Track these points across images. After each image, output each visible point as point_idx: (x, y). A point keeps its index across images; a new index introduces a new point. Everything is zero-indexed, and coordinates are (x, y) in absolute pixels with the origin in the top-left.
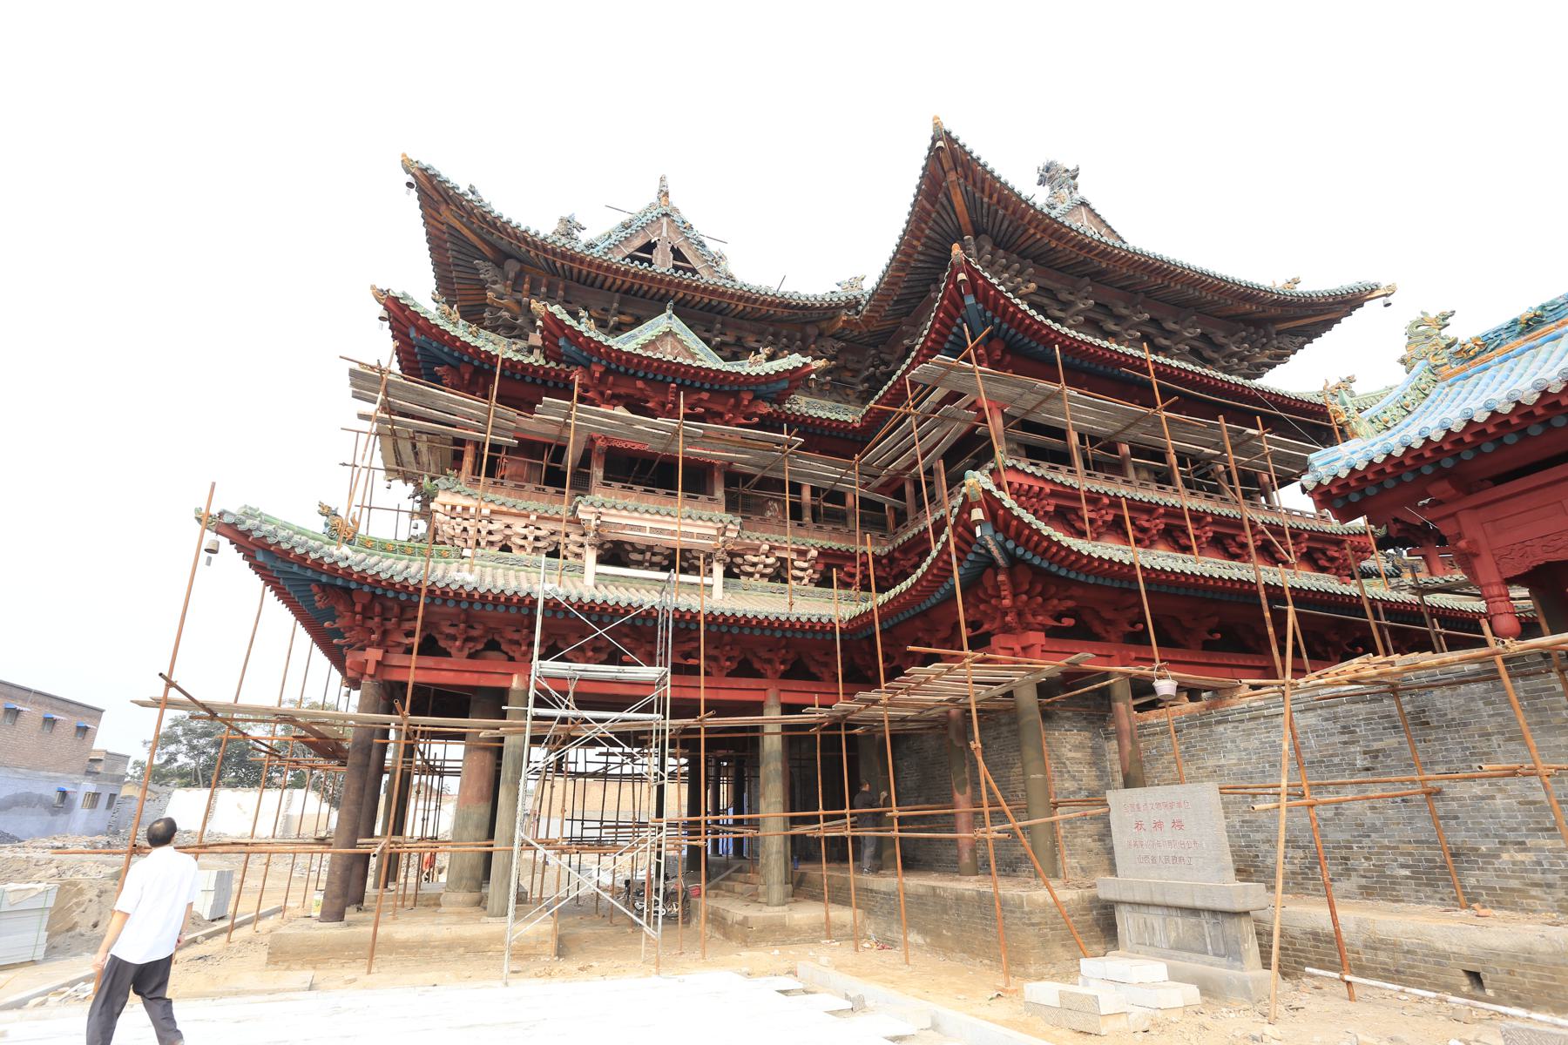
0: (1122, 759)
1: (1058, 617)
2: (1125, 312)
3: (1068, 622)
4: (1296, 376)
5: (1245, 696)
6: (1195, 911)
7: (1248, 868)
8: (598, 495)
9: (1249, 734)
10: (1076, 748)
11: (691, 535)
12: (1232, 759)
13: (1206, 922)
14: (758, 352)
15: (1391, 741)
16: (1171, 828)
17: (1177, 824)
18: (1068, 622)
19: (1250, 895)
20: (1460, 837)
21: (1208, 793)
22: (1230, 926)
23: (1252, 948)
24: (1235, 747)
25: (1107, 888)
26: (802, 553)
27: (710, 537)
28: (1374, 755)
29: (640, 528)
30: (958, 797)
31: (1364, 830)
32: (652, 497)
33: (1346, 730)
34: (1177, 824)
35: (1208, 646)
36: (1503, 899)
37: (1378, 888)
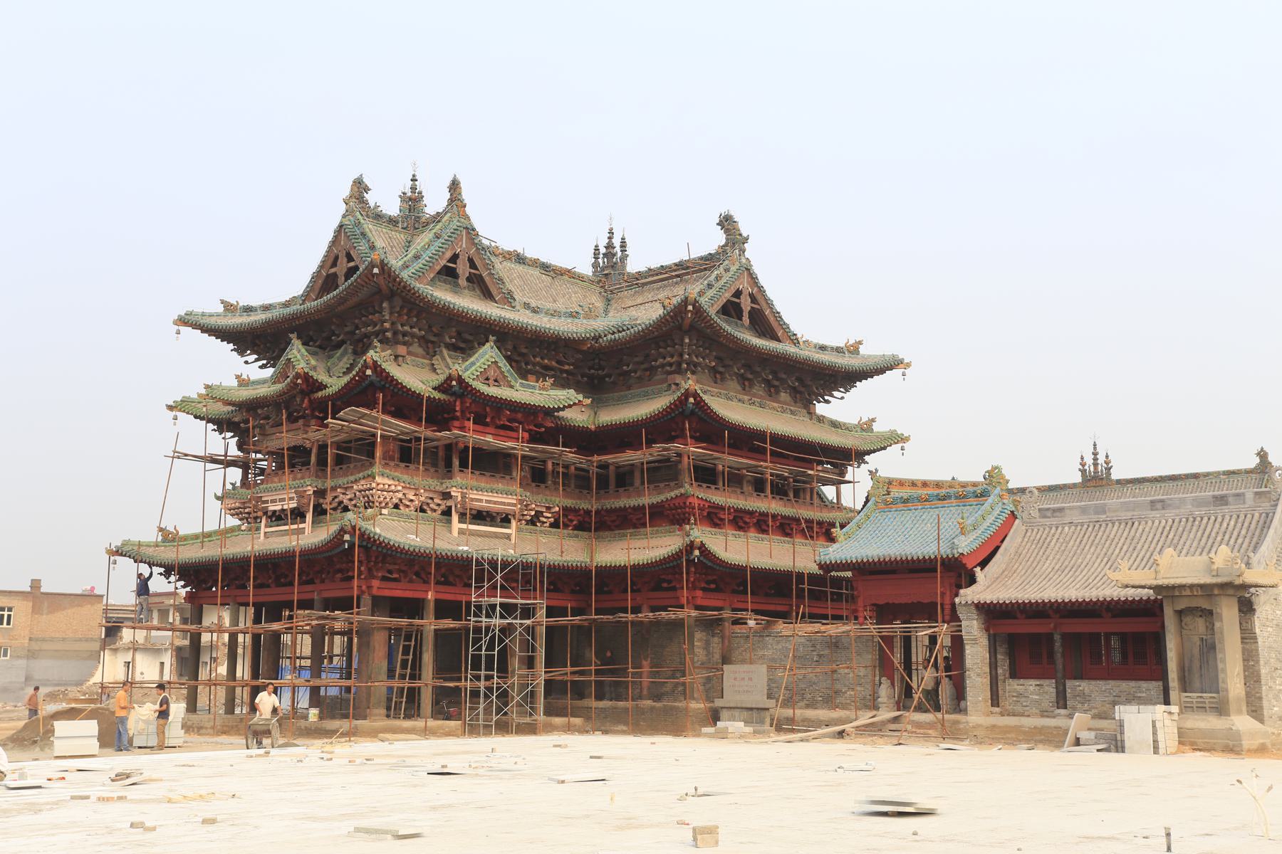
0: (722, 649)
1: (708, 582)
2: (758, 369)
3: (713, 586)
4: (843, 408)
5: (781, 627)
6: (751, 709)
7: (770, 697)
8: (459, 479)
9: (778, 642)
10: (699, 640)
11: (504, 504)
12: (768, 653)
13: (755, 714)
15: (826, 652)
16: (746, 681)
17: (750, 679)
18: (713, 586)
19: (771, 703)
20: (838, 686)
21: (762, 669)
22: (763, 713)
23: (768, 721)
24: (772, 648)
25: (718, 703)
26: (548, 508)
27: (509, 504)
28: (820, 656)
29: (481, 501)
30: (644, 663)
31: (812, 684)
32: (484, 478)
33: (813, 646)
34: (750, 679)
35: (767, 595)
36: (844, 707)
37: (812, 705)
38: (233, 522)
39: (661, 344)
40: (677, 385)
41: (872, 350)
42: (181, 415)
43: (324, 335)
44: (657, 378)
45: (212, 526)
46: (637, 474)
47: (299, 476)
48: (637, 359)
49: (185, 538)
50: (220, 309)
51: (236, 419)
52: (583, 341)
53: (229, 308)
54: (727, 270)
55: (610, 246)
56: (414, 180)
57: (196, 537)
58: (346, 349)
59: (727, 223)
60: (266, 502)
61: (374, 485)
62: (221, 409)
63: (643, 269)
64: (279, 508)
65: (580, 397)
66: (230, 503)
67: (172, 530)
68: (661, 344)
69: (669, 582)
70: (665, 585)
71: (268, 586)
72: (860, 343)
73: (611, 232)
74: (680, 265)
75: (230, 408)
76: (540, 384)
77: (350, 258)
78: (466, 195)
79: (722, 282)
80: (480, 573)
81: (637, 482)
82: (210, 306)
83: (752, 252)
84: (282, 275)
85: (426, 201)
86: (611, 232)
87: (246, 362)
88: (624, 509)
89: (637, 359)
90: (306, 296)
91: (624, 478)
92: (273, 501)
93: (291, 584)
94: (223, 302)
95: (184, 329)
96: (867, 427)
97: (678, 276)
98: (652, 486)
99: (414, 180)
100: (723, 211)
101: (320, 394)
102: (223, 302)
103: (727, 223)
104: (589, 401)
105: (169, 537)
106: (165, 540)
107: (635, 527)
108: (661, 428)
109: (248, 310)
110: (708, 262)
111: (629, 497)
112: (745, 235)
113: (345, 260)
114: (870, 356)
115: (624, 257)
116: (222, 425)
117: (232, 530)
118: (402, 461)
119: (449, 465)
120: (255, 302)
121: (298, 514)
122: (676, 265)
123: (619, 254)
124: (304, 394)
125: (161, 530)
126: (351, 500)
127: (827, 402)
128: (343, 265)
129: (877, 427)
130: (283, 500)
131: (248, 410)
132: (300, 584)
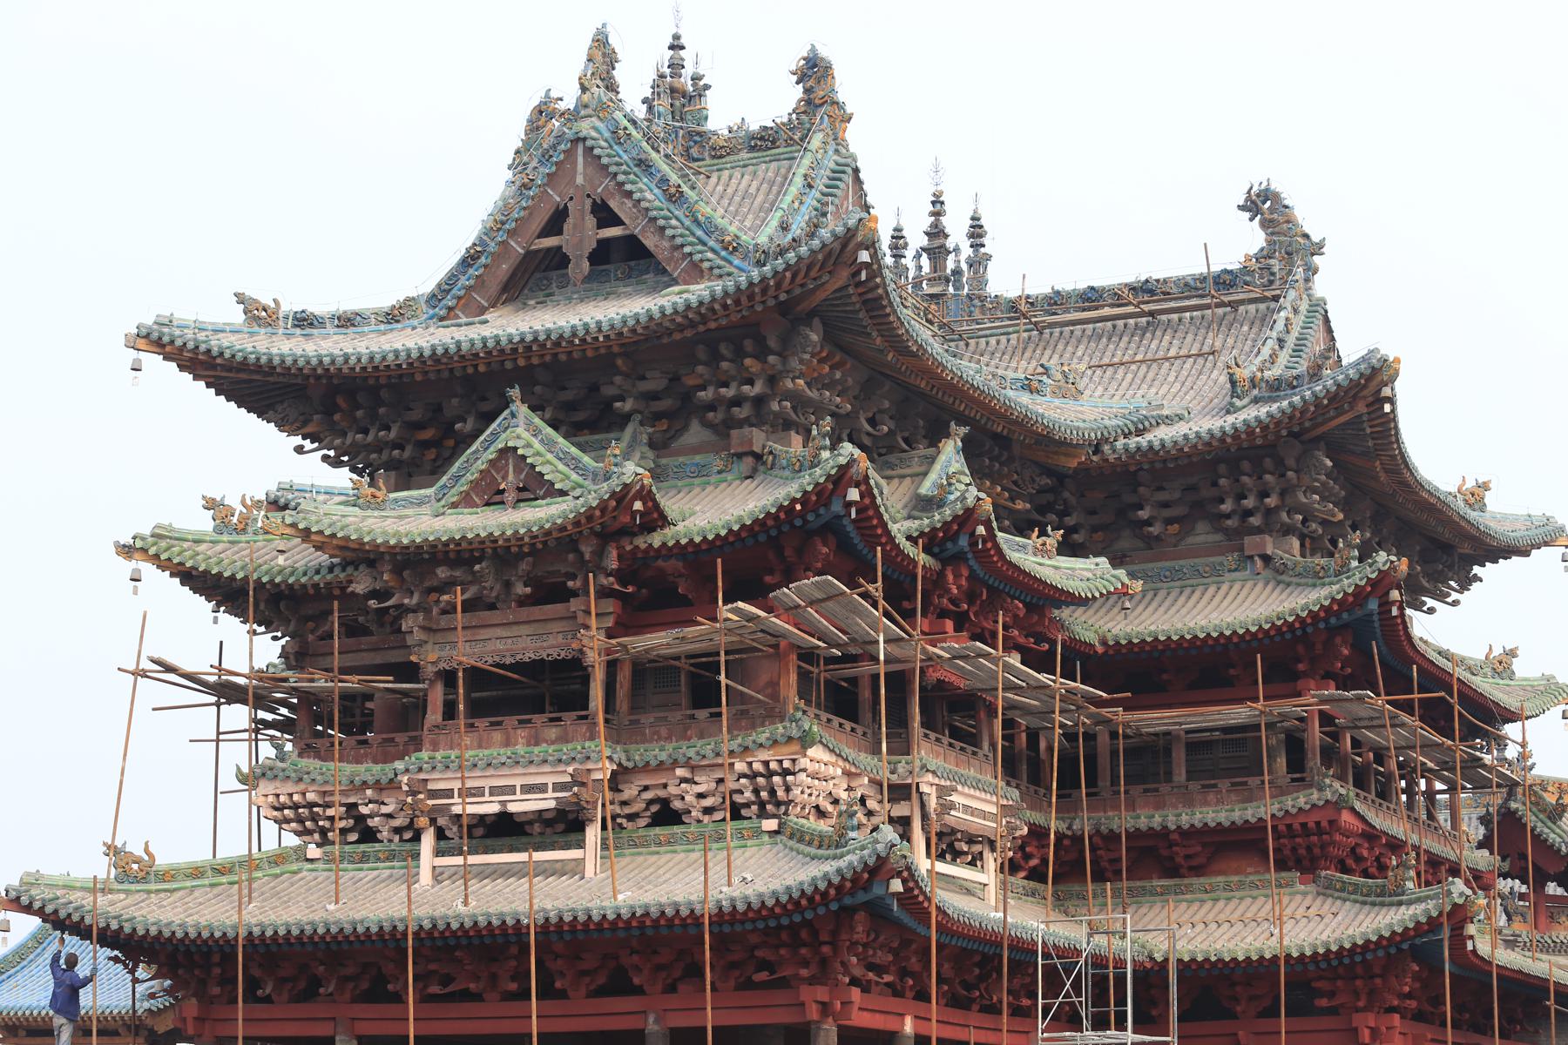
14: (1043, 533)
27: (984, 815)
38: (274, 838)
39: (1246, 465)
40: (1267, 559)
41: (1504, 508)
42: (148, 569)
43: (568, 395)
44: (1190, 540)
45: (233, 846)
46: (1179, 756)
47: (553, 732)
48: (1163, 496)
49: (167, 875)
50: (237, 316)
51: (359, 588)
52: (1063, 446)
53: (259, 314)
54: (1296, 311)
55: (936, 232)
56: (676, 46)
57: (196, 872)
58: (634, 438)
59: (1263, 205)
60: (448, 793)
61: (804, 762)
62: (292, 560)
63: (1039, 287)
64: (493, 808)
65: (1121, 573)
66: (286, 790)
67: (139, 852)
68: (1246, 465)
69: (1332, 994)
70: (1324, 1002)
71: (477, 997)
72: (1485, 486)
73: (937, 201)
74: (1146, 289)
75: (323, 558)
76: (1035, 540)
77: (604, 215)
78: (846, 88)
79: (1295, 334)
80: (1050, 971)
81: (1180, 775)
82: (212, 311)
83: (1331, 282)
84: (384, 246)
85: (712, 100)
86: (937, 201)
87: (299, 450)
88: (1164, 832)
89: (1163, 496)
90: (450, 299)
91: (1148, 762)
92: (466, 793)
93: (399, 998)
94: (241, 298)
95: (154, 362)
96: (1502, 665)
97: (1152, 314)
98: (1137, 790)
99: (676, 46)
100: (1257, 178)
101: (656, 540)
102: (241, 298)
103: (1263, 205)
104: (1138, 586)
105: (133, 870)
106: (125, 876)
107: (1172, 871)
108: (1283, 655)
109: (304, 321)
110: (1218, 296)
111: (1159, 806)
112: (1315, 238)
113: (591, 221)
114: (1505, 517)
115: (979, 262)
116: (224, 592)
117: (278, 859)
118: (698, 704)
119: (899, 721)
120: (320, 306)
121: (565, 825)
122: (1133, 289)
123: (966, 251)
124: (607, 536)
125: (112, 850)
126: (701, 796)
127: (1431, 611)
128: (582, 235)
129: (1521, 668)
130: (494, 791)
131: (398, 570)
132: (424, 999)
